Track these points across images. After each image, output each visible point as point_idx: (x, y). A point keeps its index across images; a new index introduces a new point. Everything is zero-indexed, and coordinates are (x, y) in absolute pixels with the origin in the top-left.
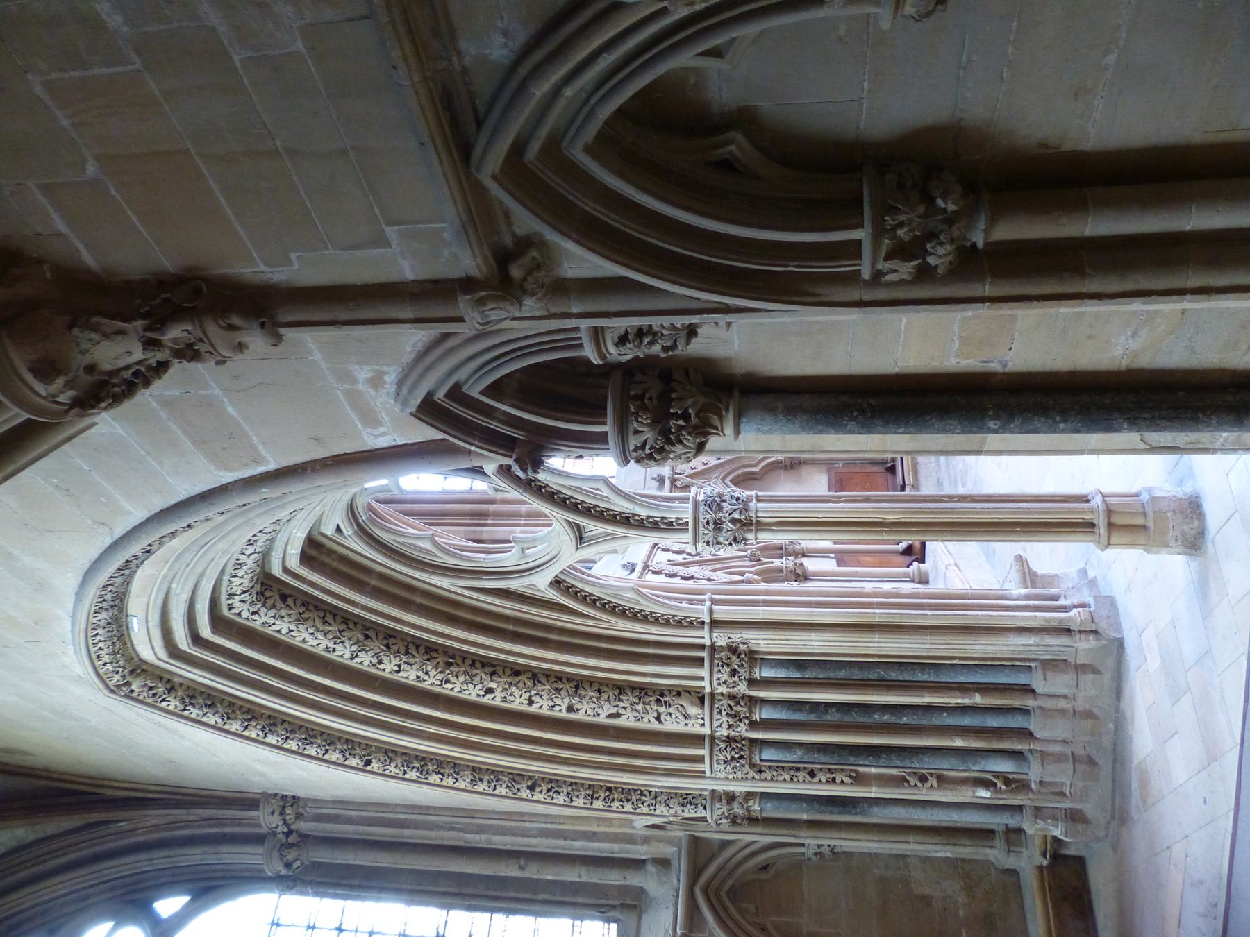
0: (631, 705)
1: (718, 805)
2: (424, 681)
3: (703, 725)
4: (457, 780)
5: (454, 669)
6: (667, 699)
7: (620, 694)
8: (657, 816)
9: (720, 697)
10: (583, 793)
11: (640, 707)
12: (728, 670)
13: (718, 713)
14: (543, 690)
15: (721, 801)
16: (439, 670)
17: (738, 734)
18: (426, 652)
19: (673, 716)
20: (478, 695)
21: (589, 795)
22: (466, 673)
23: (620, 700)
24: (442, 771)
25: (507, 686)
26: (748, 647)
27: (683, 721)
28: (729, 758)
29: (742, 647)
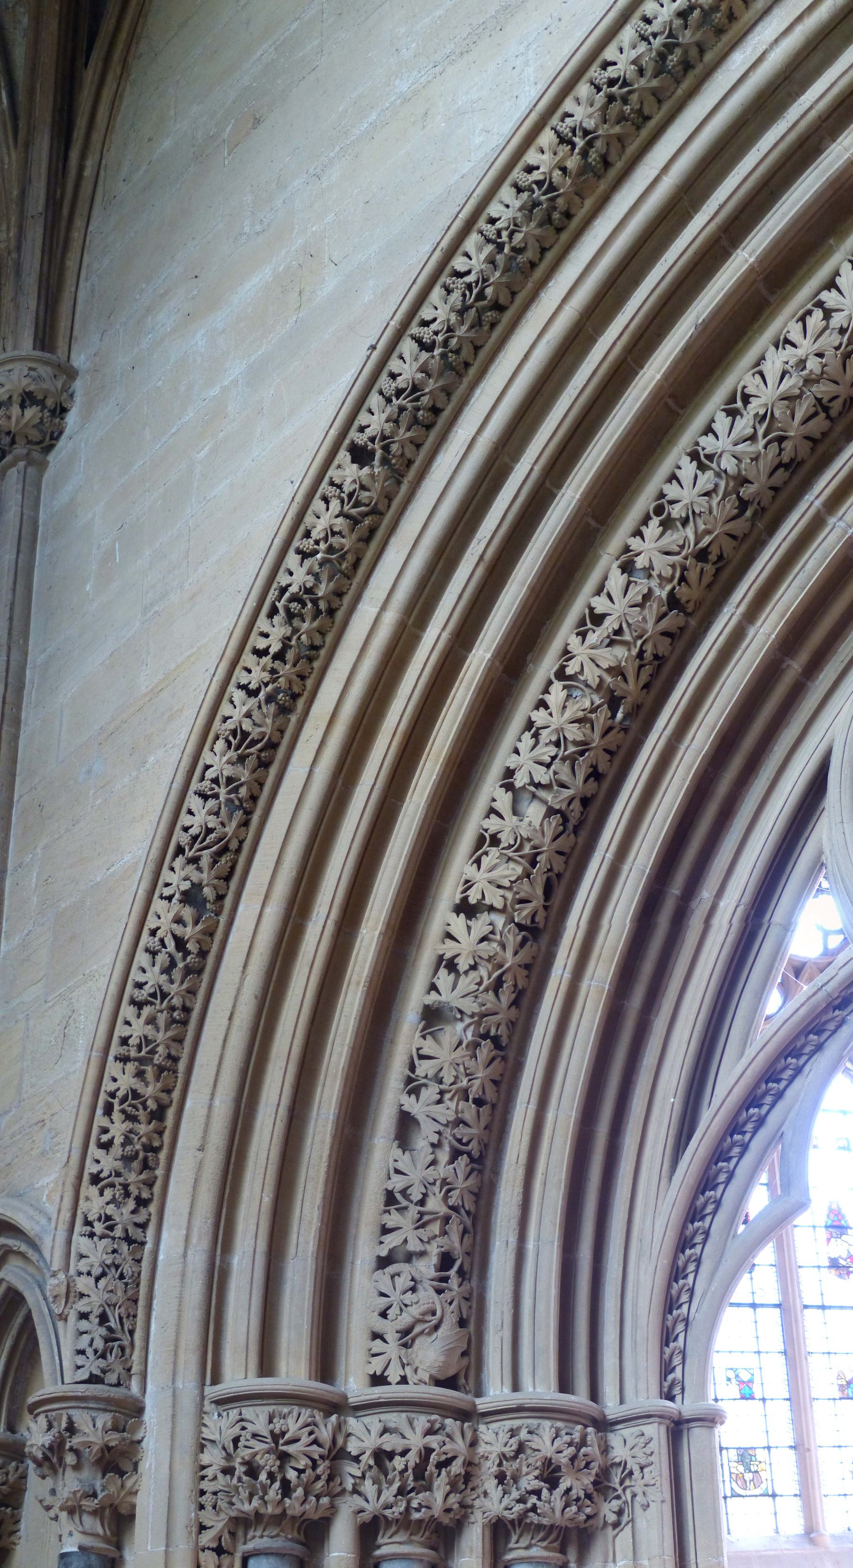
0: (444, 1182)
1: (104, 1419)
2: (583, 635)
3: (378, 1380)
4: (253, 693)
5: (601, 718)
6: (454, 1282)
7: (469, 1154)
8: (69, 1242)
9: (469, 1435)
10: (161, 1036)
11: (434, 1204)
12: (563, 1459)
13: (432, 1423)
14: (503, 946)
15: (115, 1428)
16: (608, 679)
17: (349, 1483)
18: (656, 657)
19: (409, 1297)
20: (509, 773)
21: (153, 1052)
22: (584, 747)
23: (455, 1155)
24: (290, 655)
25: (527, 850)
26: (605, 1524)
27: (389, 1329)
28: (291, 1449)
29: (608, 1510)
